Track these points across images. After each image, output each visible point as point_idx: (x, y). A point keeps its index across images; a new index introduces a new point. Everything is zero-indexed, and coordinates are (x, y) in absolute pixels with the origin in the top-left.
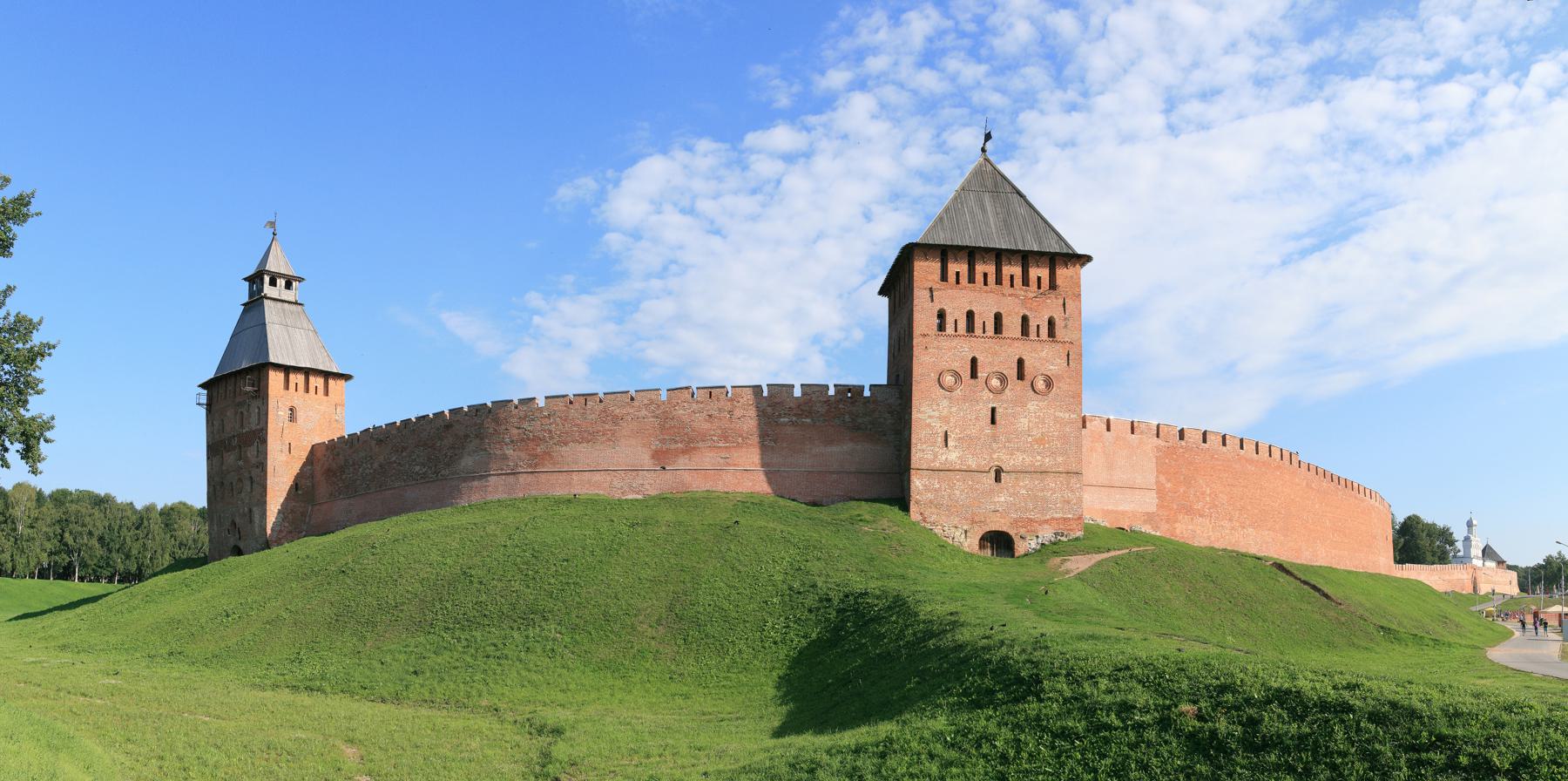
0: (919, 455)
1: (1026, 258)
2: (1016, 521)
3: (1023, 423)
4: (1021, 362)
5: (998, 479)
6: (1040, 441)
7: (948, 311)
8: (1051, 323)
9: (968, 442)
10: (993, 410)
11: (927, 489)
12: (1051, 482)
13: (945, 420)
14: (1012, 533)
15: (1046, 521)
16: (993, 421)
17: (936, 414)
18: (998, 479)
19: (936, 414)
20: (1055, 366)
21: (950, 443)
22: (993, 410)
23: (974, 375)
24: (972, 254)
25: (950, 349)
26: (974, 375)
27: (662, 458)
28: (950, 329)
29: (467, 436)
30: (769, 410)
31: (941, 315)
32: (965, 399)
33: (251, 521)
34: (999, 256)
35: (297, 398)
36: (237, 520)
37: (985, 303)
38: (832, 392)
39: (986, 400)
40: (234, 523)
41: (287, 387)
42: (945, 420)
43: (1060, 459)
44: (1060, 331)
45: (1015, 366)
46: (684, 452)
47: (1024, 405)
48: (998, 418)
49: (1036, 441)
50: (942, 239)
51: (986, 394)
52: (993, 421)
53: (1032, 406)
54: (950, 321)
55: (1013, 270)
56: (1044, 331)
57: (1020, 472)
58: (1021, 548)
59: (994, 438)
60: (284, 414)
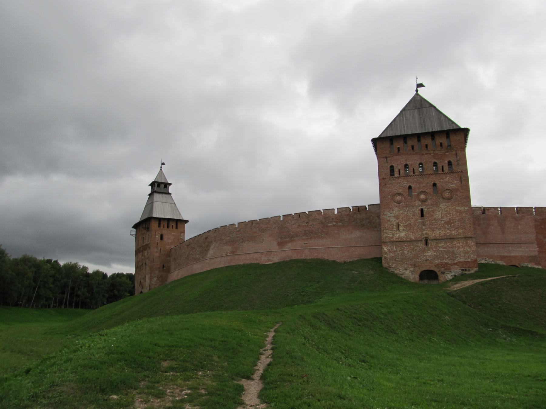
0: (386, 235)
1: (433, 135)
2: (438, 264)
3: (438, 215)
4: (435, 185)
5: (426, 244)
6: (449, 223)
7: (395, 165)
8: (450, 163)
9: (409, 227)
10: (422, 210)
11: (390, 251)
12: (456, 243)
13: (397, 217)
14: (436, 270)
15: (455, 264)
16: (422, 215)
17: (392, 215)
18: (426, 244)
19: (392, 215)
20: (454, 184)
21: (401, 228)
22: (422, 210)
23: (410, 195)
24: (405, 138)
25: (398, 183)
26: (410, 195)
27: (281, 244)
28: (396, 175)
29: (212, 242)
30: (324, 221)
31: (392, 169)
32: (406, 206)
33: (145, 281)
34: (419, 136)
35: (165, 231)
36: (142, 281)
37: (414, 161)
38: (336, 212)
39: (417, 206)
40: (141, 282)
41: (159, 226)
42: (397, 217)
43: (461, 231)
44: (455, 167)
45: (431, 187)
46: (289, 242)
47: (437, 206)
48: (424, 213)
49: (445, 223)
50: (391, 134)
51: (418, 203)
52: (422, 215)
53: (443, 206)
54: (396, 170)
55: (428, 141)
56: (446, 168)
57: (438, 240)
58: (442, 278)
59: (423, 224)
60: (158, 237)
